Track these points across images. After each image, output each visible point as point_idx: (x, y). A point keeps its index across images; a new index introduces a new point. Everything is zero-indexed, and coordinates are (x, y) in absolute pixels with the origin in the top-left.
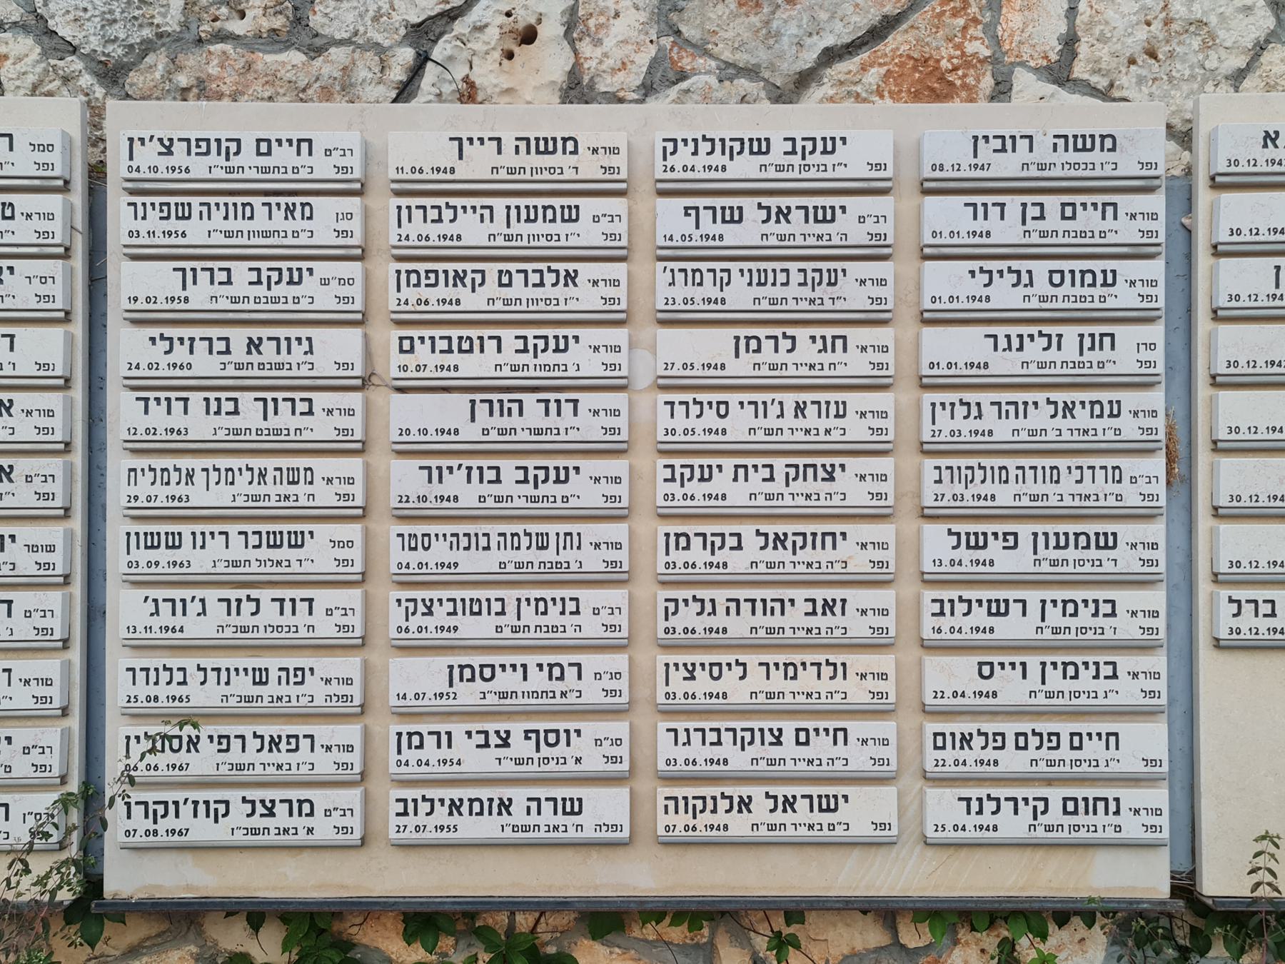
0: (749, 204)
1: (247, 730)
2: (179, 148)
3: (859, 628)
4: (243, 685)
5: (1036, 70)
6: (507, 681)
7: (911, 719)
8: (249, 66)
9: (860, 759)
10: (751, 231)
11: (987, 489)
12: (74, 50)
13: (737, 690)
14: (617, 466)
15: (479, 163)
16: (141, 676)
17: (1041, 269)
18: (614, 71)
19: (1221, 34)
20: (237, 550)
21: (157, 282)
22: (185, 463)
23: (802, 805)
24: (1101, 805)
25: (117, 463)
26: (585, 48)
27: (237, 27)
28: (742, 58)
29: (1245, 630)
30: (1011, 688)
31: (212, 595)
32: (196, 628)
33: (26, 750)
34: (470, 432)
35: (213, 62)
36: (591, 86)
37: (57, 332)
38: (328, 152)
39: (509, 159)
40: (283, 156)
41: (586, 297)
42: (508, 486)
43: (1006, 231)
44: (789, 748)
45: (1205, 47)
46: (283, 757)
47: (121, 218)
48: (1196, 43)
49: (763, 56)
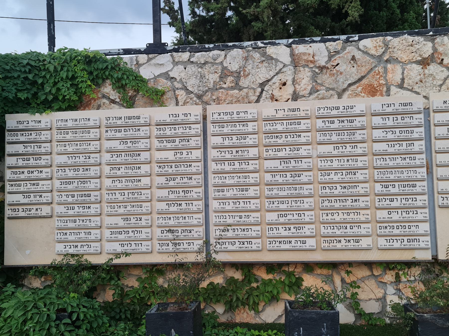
0: (336, 120)
1: (238, 228)
2: (222, 114)
3: (362, 205)
4: (237, 219)
5: (396, 86)
6: (290, 217)
7: (374, 224)
8: (227, 94)
9: (364, 232)
10: (336, 125)
11: (388, 176)
13: (337, 218)
14: (310, 173)
15: (280, 114)
16: (217, 217)
17: (398, 130)
18: (303, 91)
19: (437, 77)
20: (235, 192)
21: (217, 140)
22: (224, 175)
23: (352, 241)
24: (415, 240)
25: (211, 176)
26: (297, 86)
27: (225, 86)
28: (331, 86)
29: (445, 203)
30: (395, 216)
31: (231, 201)
32: (228, 208)
33: (196, 232)
34: (280, 167)
35: (220, 94)
36: (298, 94)
37: (199, 151)
38: (251, 114)
39: (286, 113)
40: (242, 115)
41: (303, 140)
42: (289, 178)
43: (390, 123)
44: (349, 230)
45: (433, 80)
46: (246, 233)
47: (211, 128)
48: (431, 79)
49: (335, 86)
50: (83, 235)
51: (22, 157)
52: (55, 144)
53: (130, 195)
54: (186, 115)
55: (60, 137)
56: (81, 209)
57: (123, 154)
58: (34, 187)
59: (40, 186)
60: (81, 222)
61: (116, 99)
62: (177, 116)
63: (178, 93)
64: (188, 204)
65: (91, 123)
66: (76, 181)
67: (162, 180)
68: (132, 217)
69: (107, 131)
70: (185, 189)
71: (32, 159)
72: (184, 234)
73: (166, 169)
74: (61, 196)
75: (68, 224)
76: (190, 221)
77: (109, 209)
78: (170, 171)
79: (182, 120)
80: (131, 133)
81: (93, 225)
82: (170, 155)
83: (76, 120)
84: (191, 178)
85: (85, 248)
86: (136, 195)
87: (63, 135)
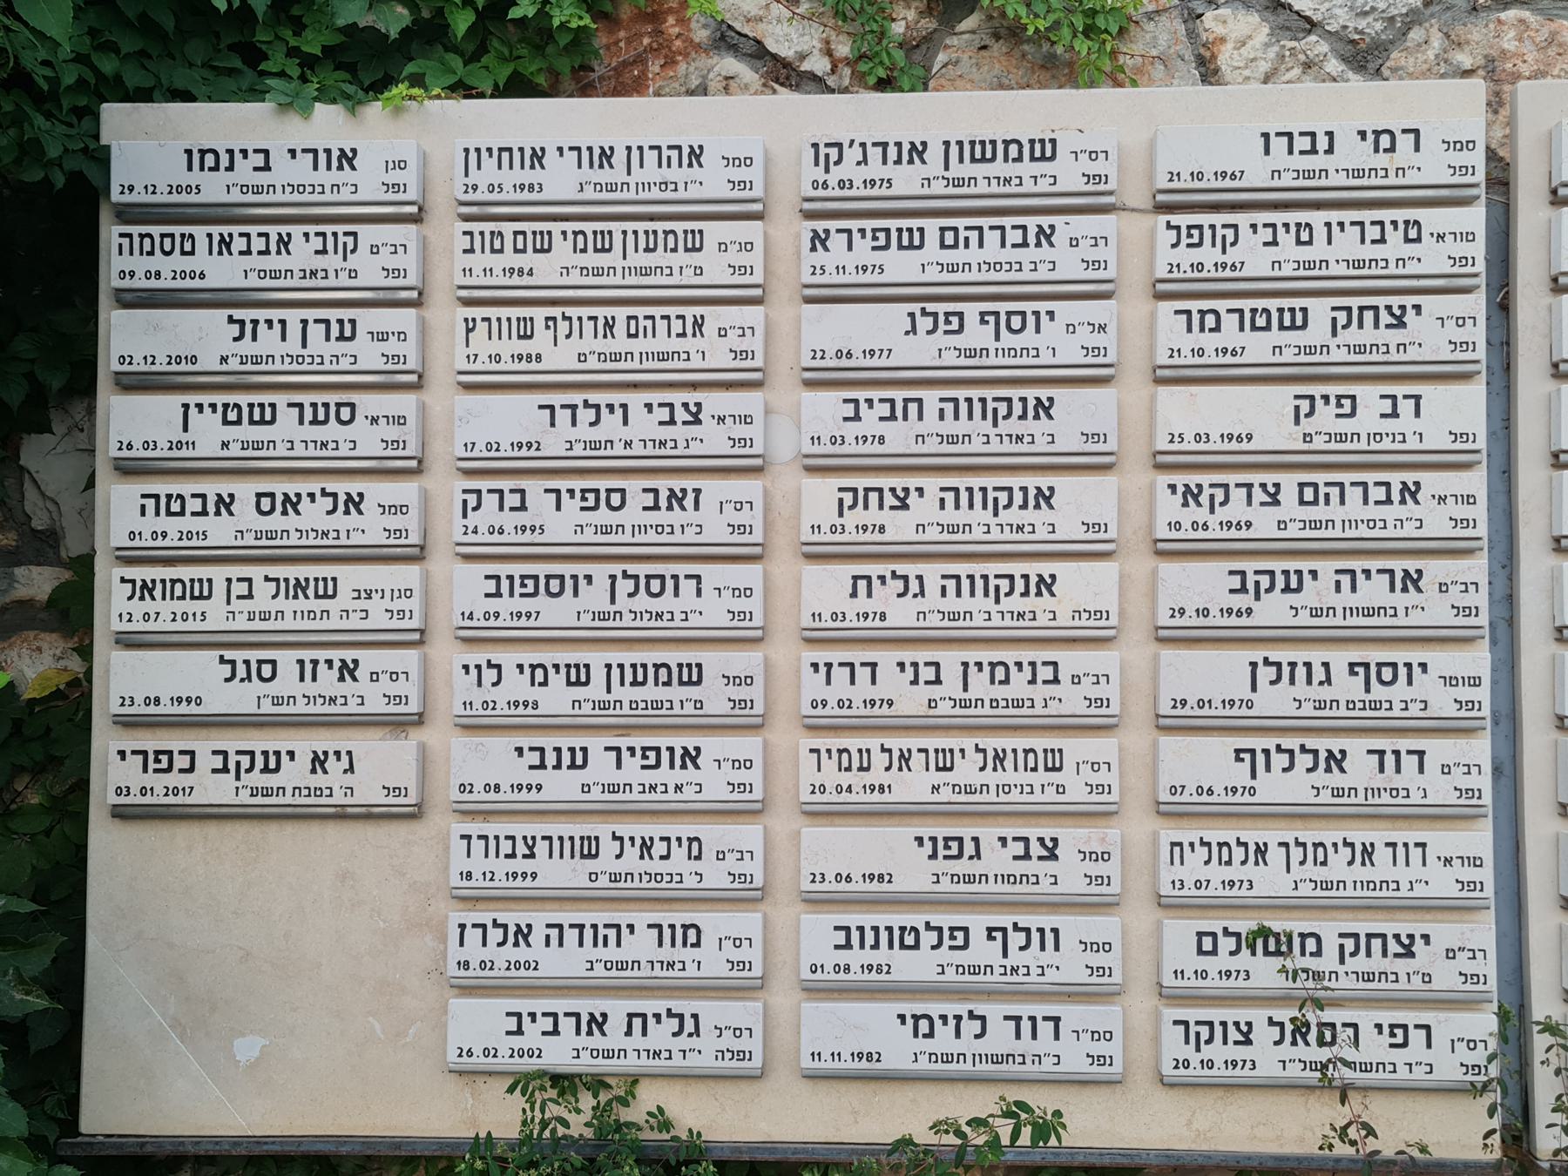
12: (1311, 25)
33: (1450, 954)
50: (640, 946)
51: (220, 399)
52: (446, 315)
53: (980, 682)
54: (1385, 141)
55: (489, 268)
56: (632, 764)
57: (931, 397)
58: (302, 604)
59: (345, 599)
60: (632, 853)
61: (803, 57)
62: (1322, 143)
63: (1220, 30)
64: (1390, 760)
65: (712, 181)
66: (601, 571)
67: (1202, 586)
68: (988, 834)
69: (819, 241)
70: (1375, 655)
71: (287, 417)
72: (1360, 963)
73: (1237, 509)
74: (490, 675)
75: (541, 863)
76: (1402, 874)
77: (831, 774)
78: (1264, 523)
79: (1358, 173)
80: (986, 256)
81: (716, 876)
82: (1266, 417)
83: (606, 156)
84: (1412, 580)
85: (661, 1035)
86: (1019, 686)
87: (509, 259)
